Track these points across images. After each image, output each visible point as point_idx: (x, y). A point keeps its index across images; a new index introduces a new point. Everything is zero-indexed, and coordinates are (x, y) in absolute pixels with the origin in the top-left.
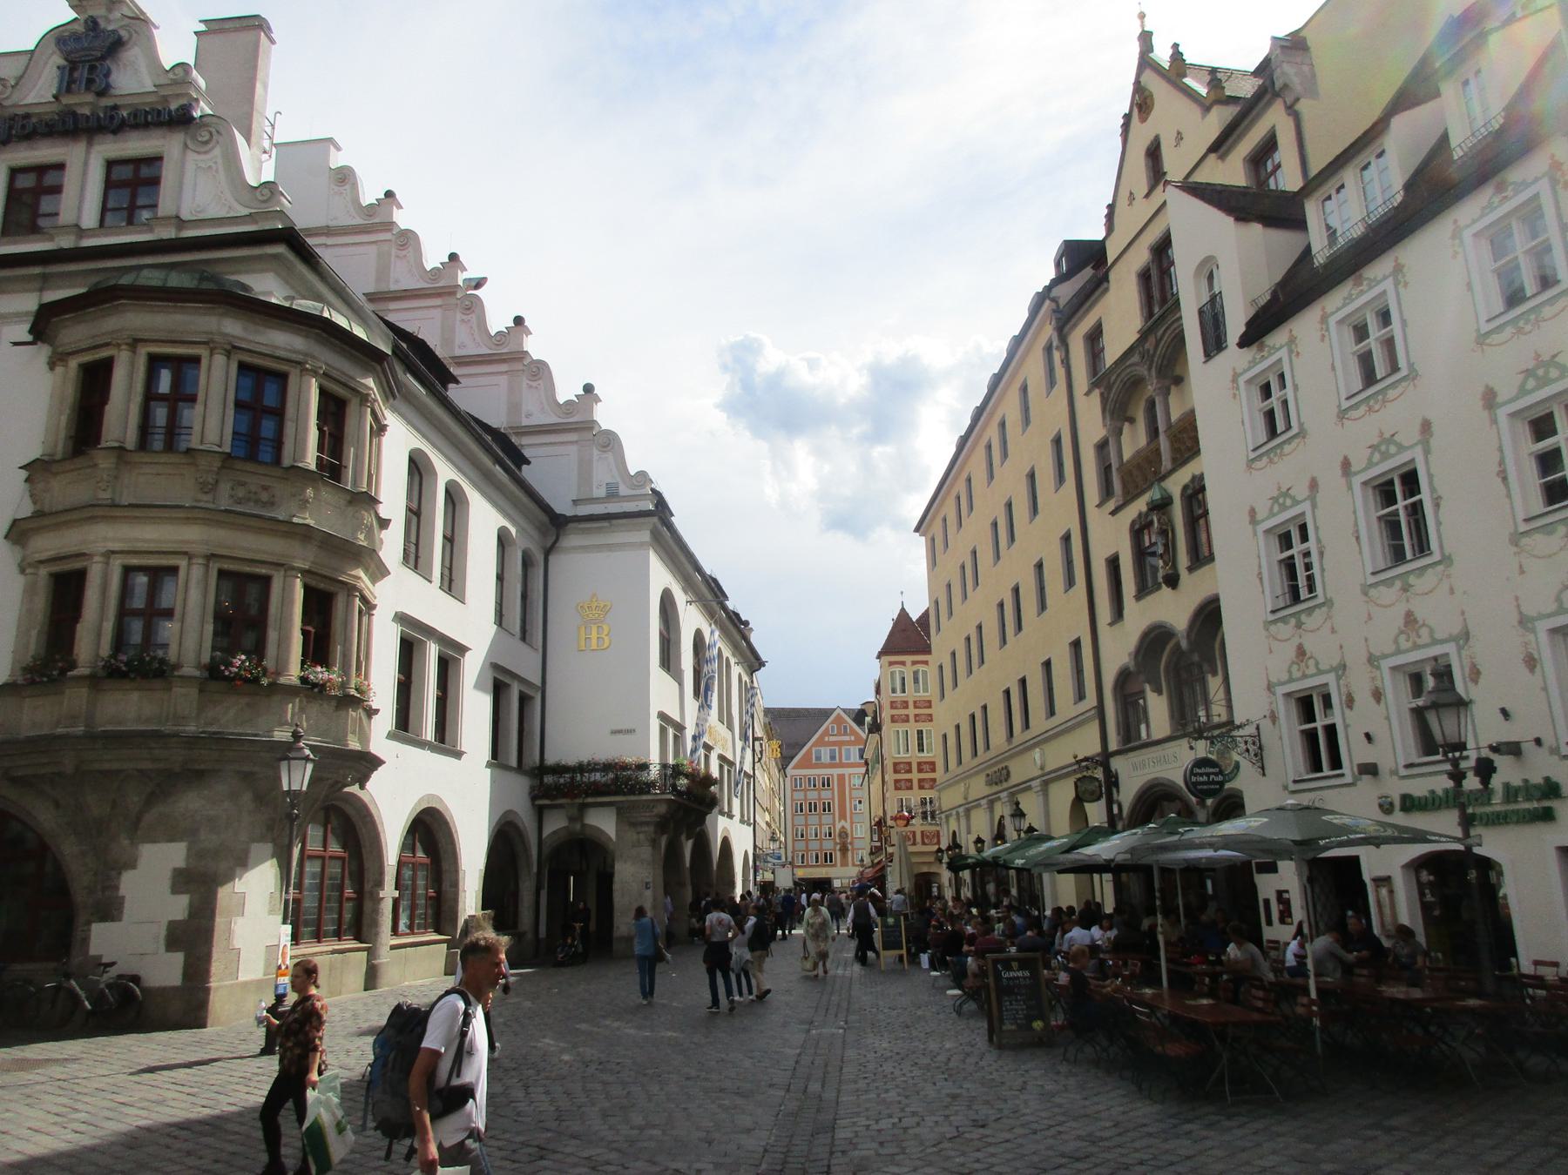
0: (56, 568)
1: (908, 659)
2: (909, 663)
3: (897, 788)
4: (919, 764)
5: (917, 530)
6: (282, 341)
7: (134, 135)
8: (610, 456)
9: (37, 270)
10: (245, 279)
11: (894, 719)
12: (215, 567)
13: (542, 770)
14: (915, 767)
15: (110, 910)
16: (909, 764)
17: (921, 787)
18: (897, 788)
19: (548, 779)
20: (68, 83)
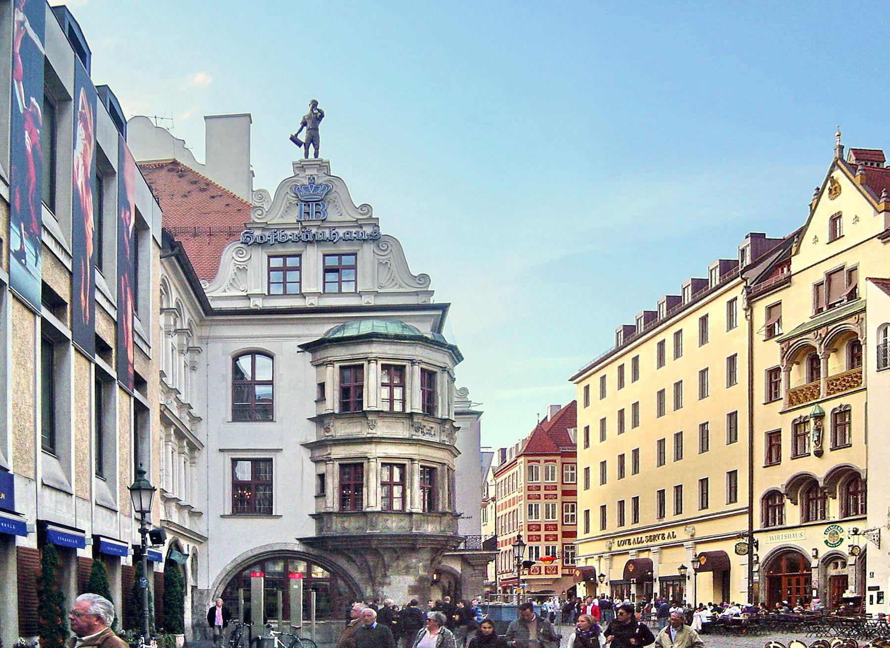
1: (542, 459)
2: (542, 461)
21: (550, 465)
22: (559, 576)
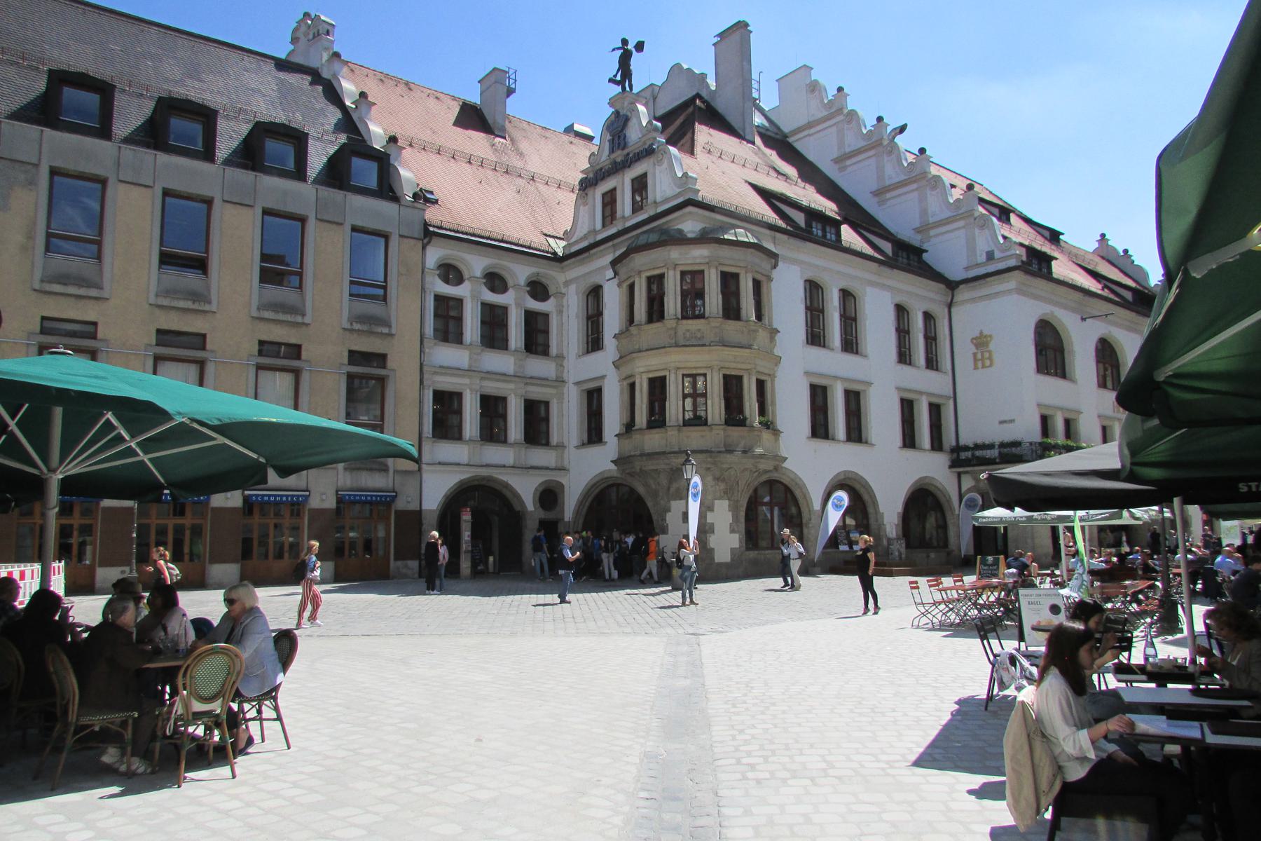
0: (631, 381)
6: (697, 255)
7: (637, 164)
8: (986, 231)
9: (610, 244)
10: (679, 227)
12: (680, 373)
13: (957, 449)
15: (664, 530)
19: (964, 455)
20: (612, 151)
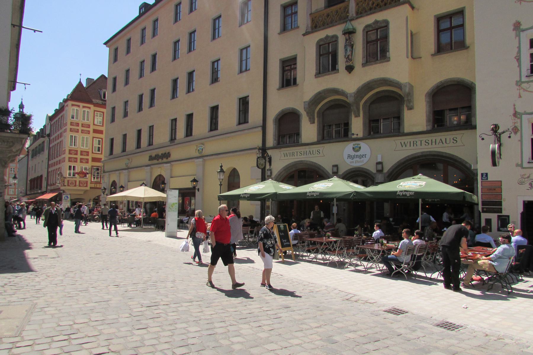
1: (82, 105)
2: (81, 106)
3: (69, 161)
4: (81, 152)
5: (105, 44)
11: (71, 130)
14: (79, 153)
16: (77, 151)
17: (81, 162)
18: (69, 161)
21: (86, 110)
22: (88, 188)
